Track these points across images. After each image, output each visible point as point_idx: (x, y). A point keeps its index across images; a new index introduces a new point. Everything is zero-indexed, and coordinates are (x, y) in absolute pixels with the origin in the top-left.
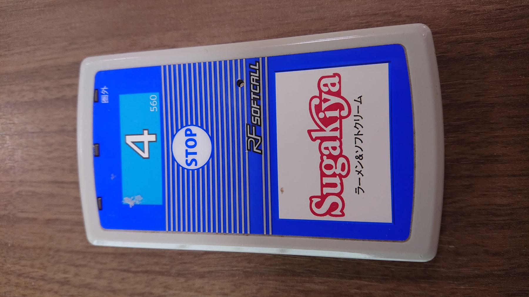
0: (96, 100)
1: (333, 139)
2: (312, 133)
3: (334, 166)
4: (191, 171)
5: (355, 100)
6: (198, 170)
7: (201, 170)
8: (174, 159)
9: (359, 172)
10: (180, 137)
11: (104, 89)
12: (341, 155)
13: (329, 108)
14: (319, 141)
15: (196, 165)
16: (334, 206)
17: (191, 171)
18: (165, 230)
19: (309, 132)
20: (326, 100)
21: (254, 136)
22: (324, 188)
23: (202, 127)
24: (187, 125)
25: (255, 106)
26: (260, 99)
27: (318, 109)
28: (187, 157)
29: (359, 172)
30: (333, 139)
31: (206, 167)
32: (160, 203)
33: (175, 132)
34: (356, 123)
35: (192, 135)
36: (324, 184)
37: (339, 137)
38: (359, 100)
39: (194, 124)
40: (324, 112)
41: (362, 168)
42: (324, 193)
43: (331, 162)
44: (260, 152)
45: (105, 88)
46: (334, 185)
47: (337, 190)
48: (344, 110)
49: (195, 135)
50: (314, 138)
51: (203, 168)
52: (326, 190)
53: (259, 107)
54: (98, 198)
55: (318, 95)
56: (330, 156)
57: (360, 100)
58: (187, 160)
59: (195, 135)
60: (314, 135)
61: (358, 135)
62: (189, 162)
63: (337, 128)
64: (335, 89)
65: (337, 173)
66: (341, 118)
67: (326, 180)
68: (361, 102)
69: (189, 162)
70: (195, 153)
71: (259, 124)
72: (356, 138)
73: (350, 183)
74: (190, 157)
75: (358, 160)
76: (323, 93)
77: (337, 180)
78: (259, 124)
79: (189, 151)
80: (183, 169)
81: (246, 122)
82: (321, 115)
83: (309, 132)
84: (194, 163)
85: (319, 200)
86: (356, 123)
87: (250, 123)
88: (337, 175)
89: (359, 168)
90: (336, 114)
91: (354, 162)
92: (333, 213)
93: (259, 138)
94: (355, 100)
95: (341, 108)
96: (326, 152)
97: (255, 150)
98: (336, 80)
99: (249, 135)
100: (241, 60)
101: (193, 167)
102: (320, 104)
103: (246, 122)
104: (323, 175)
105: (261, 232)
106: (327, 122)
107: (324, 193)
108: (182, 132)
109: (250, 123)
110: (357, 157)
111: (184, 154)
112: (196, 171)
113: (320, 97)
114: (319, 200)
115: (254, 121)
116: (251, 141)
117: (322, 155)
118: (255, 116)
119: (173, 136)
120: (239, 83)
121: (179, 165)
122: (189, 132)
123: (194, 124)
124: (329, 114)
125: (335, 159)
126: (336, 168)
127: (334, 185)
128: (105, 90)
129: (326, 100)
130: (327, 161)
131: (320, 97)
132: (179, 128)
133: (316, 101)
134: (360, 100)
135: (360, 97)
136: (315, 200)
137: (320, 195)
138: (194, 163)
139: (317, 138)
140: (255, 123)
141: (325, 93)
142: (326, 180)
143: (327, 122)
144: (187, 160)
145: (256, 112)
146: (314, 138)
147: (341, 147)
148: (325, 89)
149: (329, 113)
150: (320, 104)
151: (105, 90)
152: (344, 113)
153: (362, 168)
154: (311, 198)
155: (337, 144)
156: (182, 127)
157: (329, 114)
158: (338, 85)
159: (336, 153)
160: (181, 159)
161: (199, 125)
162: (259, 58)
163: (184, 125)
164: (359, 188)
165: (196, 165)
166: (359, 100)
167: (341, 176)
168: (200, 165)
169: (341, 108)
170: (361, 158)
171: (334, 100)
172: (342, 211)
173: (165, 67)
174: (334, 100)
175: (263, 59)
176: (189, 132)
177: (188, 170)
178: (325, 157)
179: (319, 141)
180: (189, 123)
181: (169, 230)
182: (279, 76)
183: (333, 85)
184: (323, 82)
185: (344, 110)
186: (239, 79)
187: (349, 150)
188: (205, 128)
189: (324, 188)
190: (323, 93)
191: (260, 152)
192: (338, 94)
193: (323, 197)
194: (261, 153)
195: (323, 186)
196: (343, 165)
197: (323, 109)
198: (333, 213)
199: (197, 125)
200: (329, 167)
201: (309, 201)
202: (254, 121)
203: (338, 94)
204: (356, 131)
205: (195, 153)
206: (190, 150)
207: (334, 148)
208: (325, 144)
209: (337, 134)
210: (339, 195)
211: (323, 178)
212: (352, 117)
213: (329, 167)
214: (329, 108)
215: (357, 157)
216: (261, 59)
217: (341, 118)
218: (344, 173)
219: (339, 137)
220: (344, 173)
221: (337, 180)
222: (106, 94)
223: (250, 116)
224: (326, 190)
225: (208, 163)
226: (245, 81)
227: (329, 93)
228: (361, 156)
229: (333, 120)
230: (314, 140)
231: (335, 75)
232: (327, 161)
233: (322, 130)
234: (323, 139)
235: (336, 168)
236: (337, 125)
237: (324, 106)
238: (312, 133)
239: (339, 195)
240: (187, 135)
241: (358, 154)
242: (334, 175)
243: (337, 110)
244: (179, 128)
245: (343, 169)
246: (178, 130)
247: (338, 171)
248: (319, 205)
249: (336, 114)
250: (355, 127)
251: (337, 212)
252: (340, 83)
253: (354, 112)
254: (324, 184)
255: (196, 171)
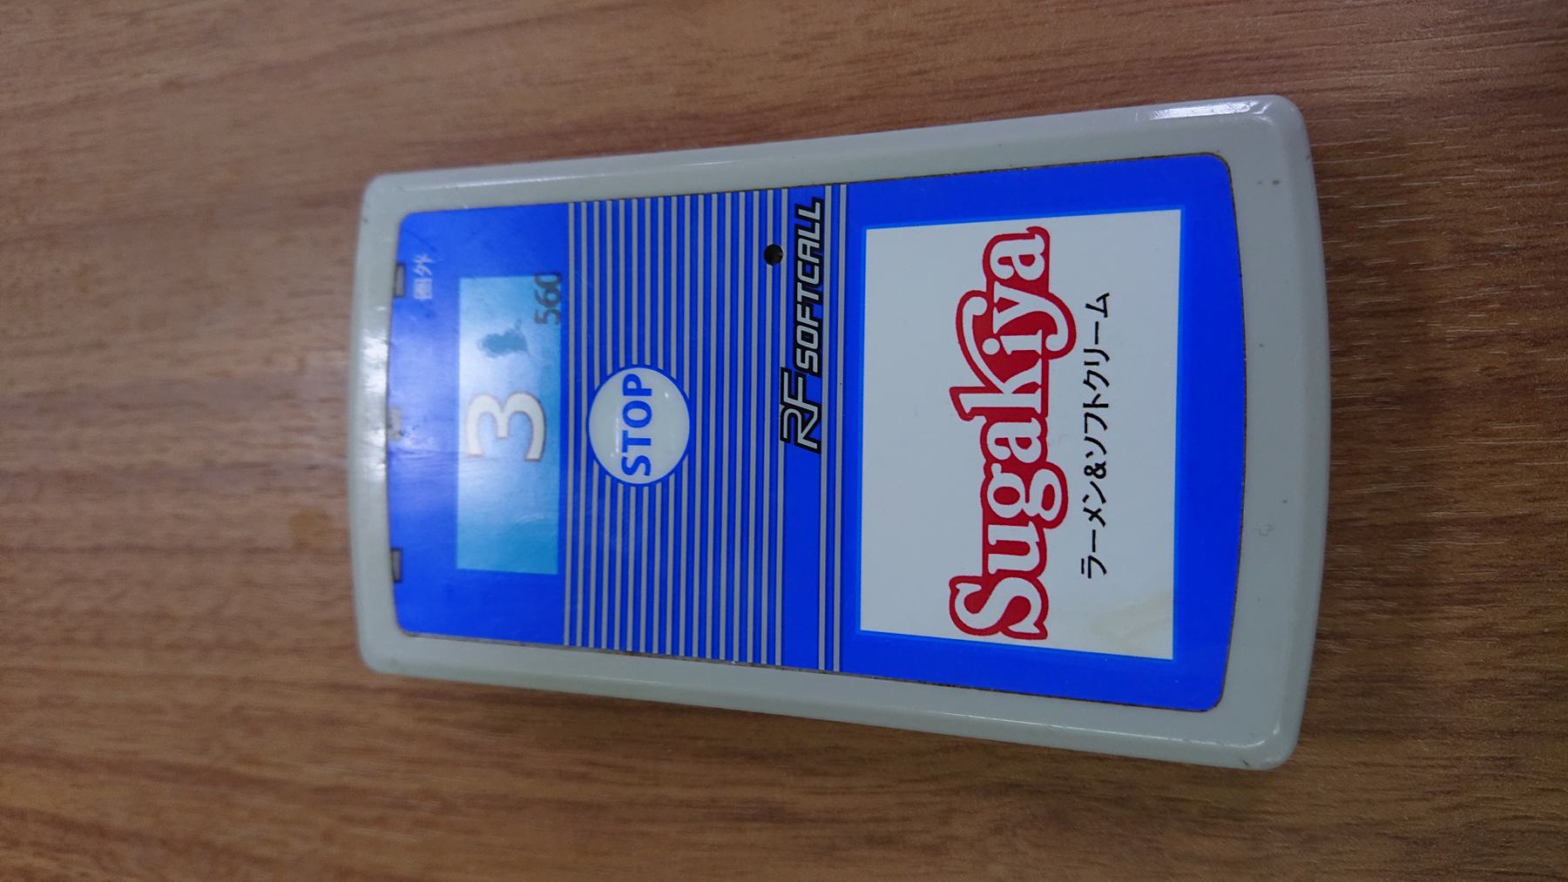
0: (399, 291)
1: (1022, 415)
2: (962, 397)
3: (1022, 494)
4: (633, 490)
5: (1088, 306)
6: (652, 486)
7: (659, 486)
8: (591, 456)
9: (1094, 514)
10: (611, 397)
11: (421, 262)
12: (1042, 463)
13: (1014, 328)
14: (981, 420)
15: (647, 473)
16: (1018, 608)
17: (633, 490)
18: (562, 643)
19: (955, 392)
20: (1005, 304)
21: (799, 403)
22: (991, 556)
23: (666, 372)
24: (629, 365)
25: (807, 320)
26: (821, 302)
27: (983, 327)
28: (625, 450)
29: (1094, 514)
30: (1022, 415)
31: (672, 478)
32: (552, 570)
33: (597, 383)
34: (1090, 372)
35: (641, 391)
36: (992, 542)
37: (1039, 411)
38: (1100, 305)
39: (648, 362)
40: (997, 337)
41: (1104, 501)
42: (992, 570)
43: (1014, 481)
44: (814, 446)
45: (425, 259)
46: (1020, 548)
47: (1029, 562)
48: (1055, 332)
49: (648, 392)
50: (967, 410)
51: (664, 481)
52: (998, 562)
53: (816, 324)
54: (393, 549)
55: (984, 289)
56: (1011, 465)
57: (1102, 305)
58: (624, 460)
59: (648, 392)
60: (969, 402)
61: (1093, 405)
62: (630, 464)
63: (1034, 383)
64: (1031, 273)
65: (1031, 512)
66: (1048, 355)
67: (997, 533)
68: (1105, 311)
69: (630, 464)
70: (647, 442)
71: (815, 370)
72: (1087, 415)
73: (1067, 542)
74: (634, 452)
75: (1093, 478)
76: (997, 284)
77: (1028, 534)
78: (815, 370)
79: (630, 436)
80: (615, 481)
81: (783, 364)
82: (991, 346)
83: (955, 392)
84: (642, 467)
85: (977, 588)
86: (1090, 372)
87: (791, 367)
88: (1032, 519)
89: (1094, 503)
90: (1031, 342)
91: (1079, 484)
92: (1013, 628)
93: (815, 409)
94: (1088, 306)
95: (1049, 327)
96: (1001, 453)
97: (801, 440)
98: (1035, 246)
99: (787, 399)
100: (777, 192)
101: (639, 477)
102: (988, 316)
103: (783, 364)
104: (990, 518)
105: (813, 666)
106: (1007, 365)
107: (992, 570)
108: (616, 382)
109: (791, 367)
110: (1089, 471)
111: (618, 441)
112: (646, 489)
113: (988, 295)
114: (977, 588)
115: (803, 361)
116: (791, 415)
117: (990, 459)
118: (804, 349)
119: (592, 394)
120: (771, 255)
121: (603, 472)
122: (632, 385)
123: (648, 362)
124: (1013, 343)
125: (1027, 472)
126: (1027, 500)
127: (1020, 548)
128: (425, 264)
129: (1005, 304)
130: (1003, 479)
131: (988, 295)
132: (610, 371)
133: (977, 306)
134: (1102, 305)
135: (1104, 297)
136: (966, 589)
137: (979, 573)
138: (642, 467)
139: (976, 411)
140: (806, 366)
141: (1004, 282)
142: (997, 533)
144: (624, 460)
145: (807, 337)
146: (967, 410)
147: (1042, 438)
148: (1004, 272)
149: (1013, 342)
150: (988, 316)
151: (425, 264)
152: (1056, 342)
153: (1104, 501)
154: (954, 582)
155: (1031, 429)
156: (617, 369)
157: (1013, 343)
158: (1040, 261)
159: (1029, 456)
160: (610, 452)
161: (661, 366)
162: (823, 186)
163: (622, 364)
164: (1091, 558)
165: (647, 473)
166: (1100, 305)
167: (1040, 524)
168: (659, 471)
169: (1049, 327)
170: (1100, 472)
171: (1028, 303)
172: (1039, 623)
173: (577, 205)
174: (1028, 303)
175: (836, 187)
176: (632, 385)
177: (627, 486)
178: (996, 468)
179: (981, 420)
180: (635, 362)
181: (573, 643)
182: (877, 239)
183: (1027, 260)
184: (1000, 250)
185: (1055, 332)
186: (770, 242)
187: (1068, 450)
188: (674, 375)
189: (991, 556)
190: (997, 284)
191: (814, 446)
192: (1040, 287)
193: (989, 582)
194: (819, 451)
195: (988, 549)
196: (1049, 491)
197: (995, 330)
198: (1013, 628)
199: (653, 366)
200: (1007, 496)
201: (948, 592)
202: (803, 361)
203: (1040, 287)
204: (1089, 396)
205: (647, 442)
206: (634, 433)
207: (1024, 443)
208: (999, 429)
209: (1033, 401)
210: (1032, 576)
211: (991, 527)
212: (1077, 354)
213: (1007, 496)
214: (1014, 328)
215: (1089, 471)
216: (828, 189)
217: (1048, 355)
218: (1049, 515)
219: (1039, 411)
220: (1049, 515)
221: (1028, 534)
222: (426, 275)
223: (793, 345)
224: (998, 562)
225: (677, 470)
226: (784, 248)
227: (1016, 282)
228: (1101, 466)
229: (1024, 360)
230: (966, 417)
231: (1032, 233)
232: (1003, 479)
233: (990, 388)
235: (1027, 500)
236: (1033, 375)
237: (1000, 319)
238: (962, 397)
239: (1032, 576)
240: (627, 392)
241: (1092, 462)
242: (1021, 520)
243: (1035, 333)
244: (610, 371)
245: (1047, 502)
246: (604, 378)
247: (1034, 508)
248: (975, 603)
249: (1031, 342)
250: (1087, 382)
251: (1027, 625)
252: (1046, 254)
253: (1084, 338)
254: (992, 542)
255: (646, 489)
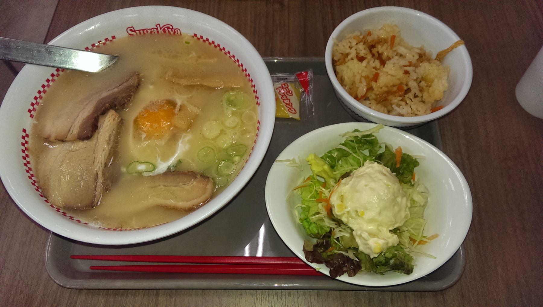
27: (168, 28)
56: (151, 32)
60: (158, 26)
82: (166, 29)
104: (143, 30)
124: (167, 31)
130: (149, 31)
133: (171, 27)
142: (142, 32)
143: (164, 30)
157: (167, 31)
171: (172, 33)
174: (172, 33)
193: (135, 31)
195: (139, 31)
213: (147, 32)
227: (175, 32)
232: (149, 31)
233: (161, 29)
234: (157, 29)
237: (170, 30)
